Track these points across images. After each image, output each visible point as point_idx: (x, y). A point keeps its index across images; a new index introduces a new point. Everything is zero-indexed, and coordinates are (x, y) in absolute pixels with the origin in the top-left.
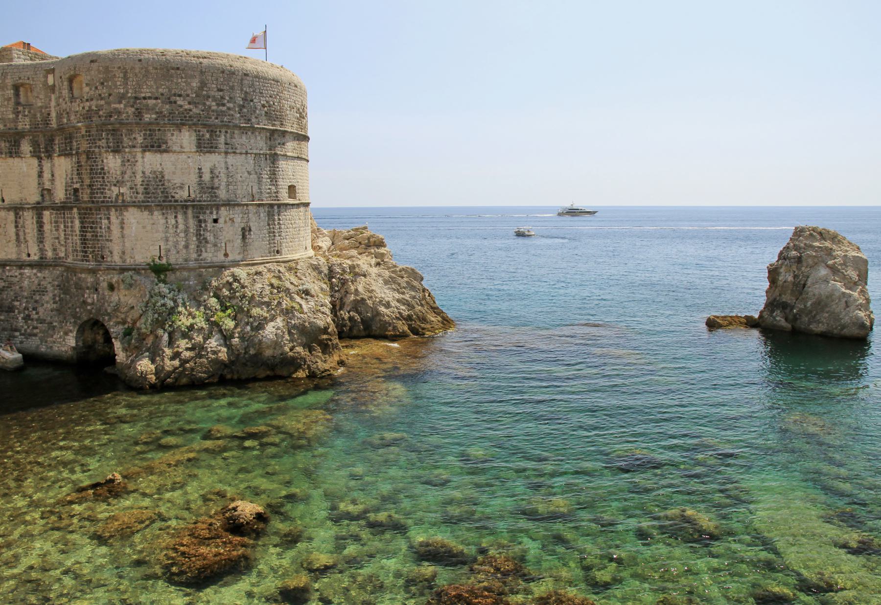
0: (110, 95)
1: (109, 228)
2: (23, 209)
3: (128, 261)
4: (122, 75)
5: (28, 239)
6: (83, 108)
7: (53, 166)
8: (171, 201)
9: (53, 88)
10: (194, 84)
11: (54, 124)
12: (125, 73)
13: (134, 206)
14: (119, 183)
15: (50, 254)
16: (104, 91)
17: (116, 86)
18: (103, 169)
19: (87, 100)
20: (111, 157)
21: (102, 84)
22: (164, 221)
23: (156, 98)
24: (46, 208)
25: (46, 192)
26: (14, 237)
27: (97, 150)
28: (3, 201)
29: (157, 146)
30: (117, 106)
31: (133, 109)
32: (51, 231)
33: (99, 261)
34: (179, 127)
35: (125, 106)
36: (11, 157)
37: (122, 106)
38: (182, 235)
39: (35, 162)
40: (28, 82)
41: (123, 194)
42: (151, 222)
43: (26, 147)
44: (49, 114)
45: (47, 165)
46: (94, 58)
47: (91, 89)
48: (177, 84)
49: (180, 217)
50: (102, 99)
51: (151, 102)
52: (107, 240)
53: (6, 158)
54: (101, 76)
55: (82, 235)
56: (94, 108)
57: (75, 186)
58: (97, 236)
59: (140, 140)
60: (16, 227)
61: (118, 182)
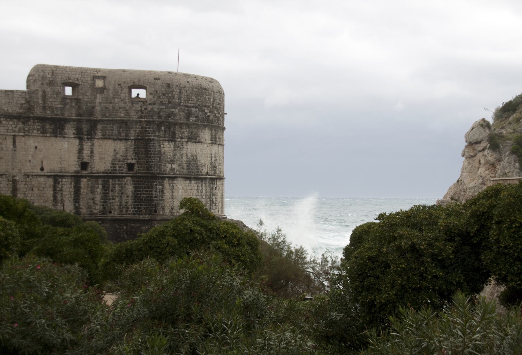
0: (170, 102)
1: (162, 191)
2: (63, 177)
3: (175, 214)
4: (178, 91)
5: (65, 199)
6: (146, 109)
7: (93, 145)
8: (200, 175)
9: (102, 90)
10: (211, 100)
11: (98, 115)
12: (180, 90)
13: (182, 177)
14: (172, 162)
15: (84, 211)
16: (165, 100)
17: (174, 97)
18: (160, 151)
19: (150, 104)
20: (166, 143)
21: (164, 95)
22: (196, 188)
23: (196, 107)
24: (85, 177)
25: (84, 166)
26: (52, 198)
27: (156, 138)
28: (42, 169)
29: (194, 139)
30: (174, 110)
31: (184, 113)
32: (87, 194)
33: (152, 215)
34: (205, 126)
35: (179, 111)
36: (56, 137)
37: (177, 111)
38: (204, 197)
39: (77, 142)
40: (77, 82)
41: (174, 168)
42: (190, 188)
43: (70, 130)
44: (93, 107)
45: (87, 145)
46: (157, 77)
47: (154, 97)
48: (205, 99)
49: (204, 185)
50: (163, 104)
51: (194, 110)
52: (162, 200)
53: (50, 137)
54: (164, 90)
55: (135, 197)
56: (156, 110)
57: (134, 161)
58: (151, 197)
59: (186, 134)
60: (55, 190)
61: (171, 161)
